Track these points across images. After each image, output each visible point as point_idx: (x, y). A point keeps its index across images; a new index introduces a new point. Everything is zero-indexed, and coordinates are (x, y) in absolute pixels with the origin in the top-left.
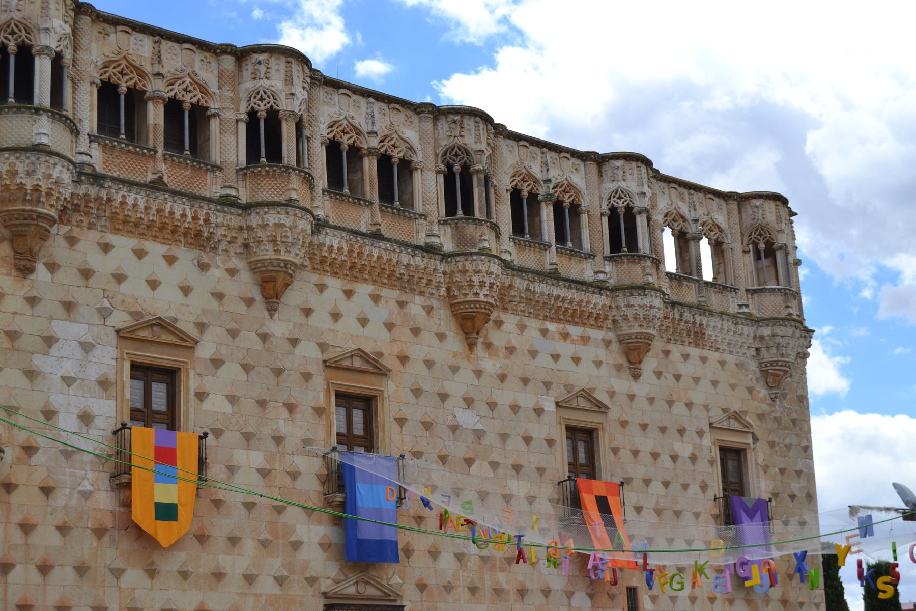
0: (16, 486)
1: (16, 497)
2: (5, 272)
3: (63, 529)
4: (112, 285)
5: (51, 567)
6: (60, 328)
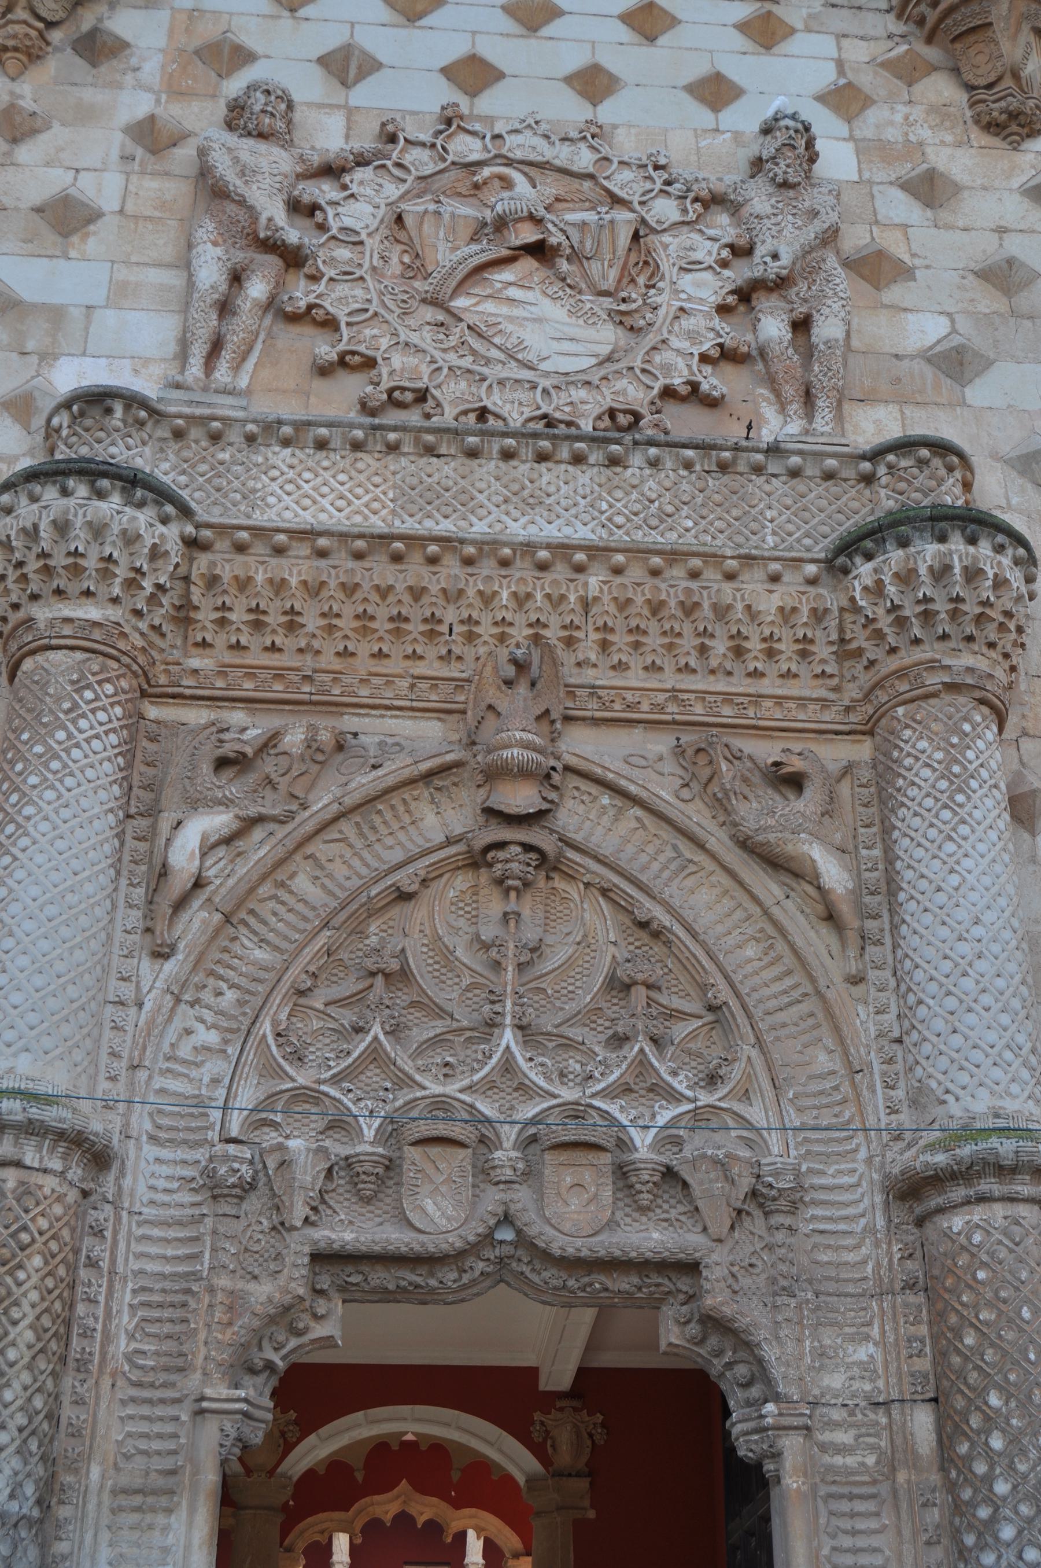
2: (949, 138)
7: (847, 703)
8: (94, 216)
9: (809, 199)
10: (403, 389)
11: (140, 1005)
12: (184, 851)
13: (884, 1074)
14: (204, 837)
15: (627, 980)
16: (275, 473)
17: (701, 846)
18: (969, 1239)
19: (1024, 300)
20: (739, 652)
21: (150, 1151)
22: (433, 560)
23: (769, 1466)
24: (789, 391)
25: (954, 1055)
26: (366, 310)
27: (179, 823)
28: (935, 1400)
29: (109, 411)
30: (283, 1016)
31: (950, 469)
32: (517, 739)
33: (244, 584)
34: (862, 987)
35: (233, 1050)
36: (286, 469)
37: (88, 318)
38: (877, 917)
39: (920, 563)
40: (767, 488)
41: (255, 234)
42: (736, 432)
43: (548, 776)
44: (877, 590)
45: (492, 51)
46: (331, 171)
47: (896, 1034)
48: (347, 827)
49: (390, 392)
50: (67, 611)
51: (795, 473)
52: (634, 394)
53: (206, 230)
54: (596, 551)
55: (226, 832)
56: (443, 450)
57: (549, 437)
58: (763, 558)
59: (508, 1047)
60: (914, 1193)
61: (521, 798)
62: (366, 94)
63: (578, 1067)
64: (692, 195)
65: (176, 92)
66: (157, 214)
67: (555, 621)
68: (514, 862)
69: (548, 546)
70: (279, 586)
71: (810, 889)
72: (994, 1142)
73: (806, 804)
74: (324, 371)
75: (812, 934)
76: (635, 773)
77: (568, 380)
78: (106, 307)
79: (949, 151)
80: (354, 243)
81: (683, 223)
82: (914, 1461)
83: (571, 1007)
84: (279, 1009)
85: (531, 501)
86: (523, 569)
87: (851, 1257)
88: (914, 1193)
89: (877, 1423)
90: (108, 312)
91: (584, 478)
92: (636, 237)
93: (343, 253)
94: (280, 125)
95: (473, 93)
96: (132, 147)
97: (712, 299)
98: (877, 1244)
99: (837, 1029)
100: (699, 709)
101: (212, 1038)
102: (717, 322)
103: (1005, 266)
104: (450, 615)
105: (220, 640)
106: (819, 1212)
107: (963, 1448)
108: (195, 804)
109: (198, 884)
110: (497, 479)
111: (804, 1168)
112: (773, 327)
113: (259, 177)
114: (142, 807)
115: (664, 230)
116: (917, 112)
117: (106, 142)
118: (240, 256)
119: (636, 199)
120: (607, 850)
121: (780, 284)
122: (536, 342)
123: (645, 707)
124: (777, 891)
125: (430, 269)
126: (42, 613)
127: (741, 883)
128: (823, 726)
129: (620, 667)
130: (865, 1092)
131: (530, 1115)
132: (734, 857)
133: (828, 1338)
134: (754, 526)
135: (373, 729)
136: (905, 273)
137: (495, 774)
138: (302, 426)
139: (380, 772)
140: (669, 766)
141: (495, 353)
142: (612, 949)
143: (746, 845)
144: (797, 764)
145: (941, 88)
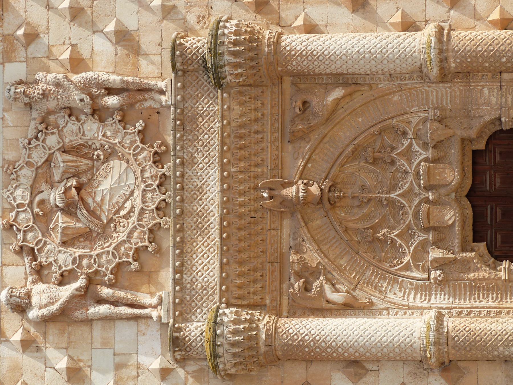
7: (271, 84)
10: (149, 238)
11: (388, 308)
12: (337, 297)
13: (401, 80)
14: (333, 292)
15: (373, 159)
16: (194, 280)
18: (458, 62)
21: (433, 300)
24: (140, 97)
25: (402, 62)
26: (113, 253)
27: (327, 301)
28: (500, 72)
29: (177, 338)
30: (388, 265)
33: (239, 287)
34: (372, 85)
36: (192, 276)
37: (119, 355)
38: (348, 79)
39: (232, 61)
40: (189, 108)
41: (82, 295)
43: (305, 184)
47: (388, 76)
48: (324, 248)
49: (150, 242)
51: (183, 99)
53: (80, 314)
55: (331, 286)
56: (181, 222)
58: (222, 112)
59: (396, 196)
63: (400, 174)
64: (44, 130)
66: (66, 335)
69: (222, 185)
71: (341, 101)
73: (314, 102)
75: (355, 100)
78: (114, 349)
79: (5, 24)
80: (80, 259)
81: (58, 134)
85: (201, 191)
87: (458, 93)
89: (506, 89)
90: (116, 347)
92: (64, 152)
93: (85, 262)
97: (97, 124)
98: (455, 86)
100: (276, 135)
103: (71, 10)
106: (444, 102)
110: (192, 203)
111: (431, 106)
113: (53, 296)
115: (63, 141)
119: (48, 152)
120: (329, 166)
123: (277, 152)
124: (341, 111)
125: (88, 230)
127: (339, 122)
128: (280, 93)
130: (408, 87)
131: (418, 189)
134: (206, 113)
138: (175, 272)
139: (305, 239)
141: (128, 205)
142: (361, 163)
144: (299, 103)
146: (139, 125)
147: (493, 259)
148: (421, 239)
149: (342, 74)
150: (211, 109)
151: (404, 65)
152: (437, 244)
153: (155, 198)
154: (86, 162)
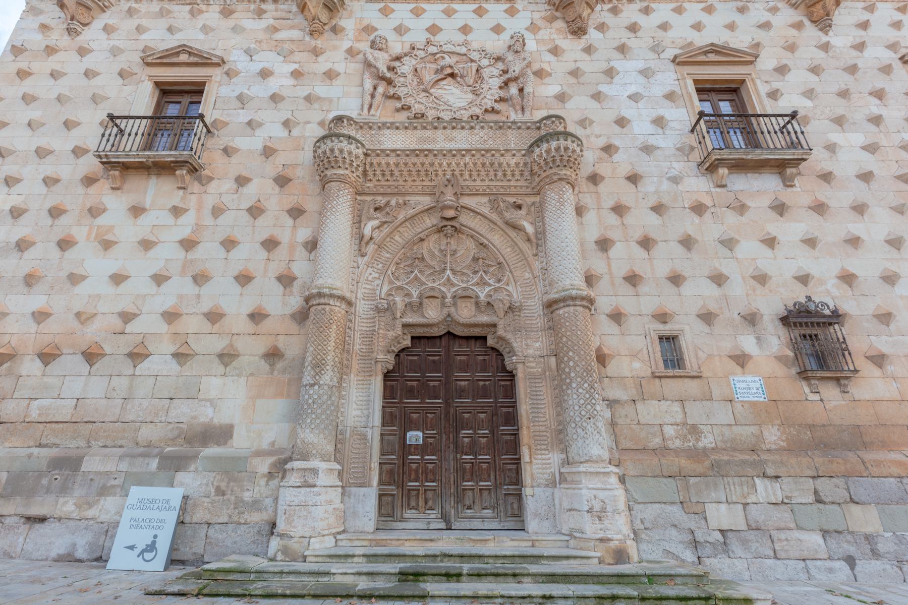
0: (603, 178)
1: (602, 187)
3: (658, 209)
4: (660, 33)
5: (655, 242)
6: (619, 64)
8: (338, 74)
9: (522, 55)
12: (367, 231)
17: (496, 224)
19: (581, 80)
20: (505, 175)
22: (426, 156)
23: (514, 372)
24: (518, 107)
31: (560, 123)
32: (449, 198)
33: (379, 164)
35: (382, 278)
42: (504, 119)
44: (540, 156)
45: (439, 23)
46: (398, 59)
48: (407, 223)
50: (335, 172)
52: (477, 111)
54: (467, 151)
57: (455, 123)
60: (550, 306)
61: (451, 213)
62: (406, 38)
65: (358, 41)
67: (457, 170)
68: (449, 230)
70: (388, 164)
72: (571, 291)
73: (523, 212)
74: (398, 110)
76: (480, 207)
77: (460, 109)
82: (550, 369)
83: (464, 265)
84: (393, 268)
86: (449, 156)
88: (550, 306)
91: (465, 133)
92: (477, 70)
93: (402, 79)
94: (384, 46)
95: (434, 35)
96: (347, 56)
99: (530, 267)
101: (377, 275)
102: (499, 91)
104: (431, 170)
105: (374, 179)
107: (563, 366)
108: (370, 219)
109: (371, 239)
112: (513, 90)
114: (358, 222)
116: (553, 31)
117: (340, 55)
118: (375, 82)
120: (472, 226)
121: (516, 79)
122: (452, 100)
126: (329, 173)
129: (475, 180)
132: (503, 226)
133: (529, 342)
135: (413, 199)
136: (550, 75)
137: (445, 207)
138: (392, 123)
140: (488, 205)
143: (507, 223)
144: (520, 202)
145: (560, 24)
146: (497, 106)
147: (397, 351)
148: (413, 293)
149: (544, 234)
150: (515, 140)
151: (557, 273)
152: (409, 306)
153: (446, 116)
154: (471, 81)
